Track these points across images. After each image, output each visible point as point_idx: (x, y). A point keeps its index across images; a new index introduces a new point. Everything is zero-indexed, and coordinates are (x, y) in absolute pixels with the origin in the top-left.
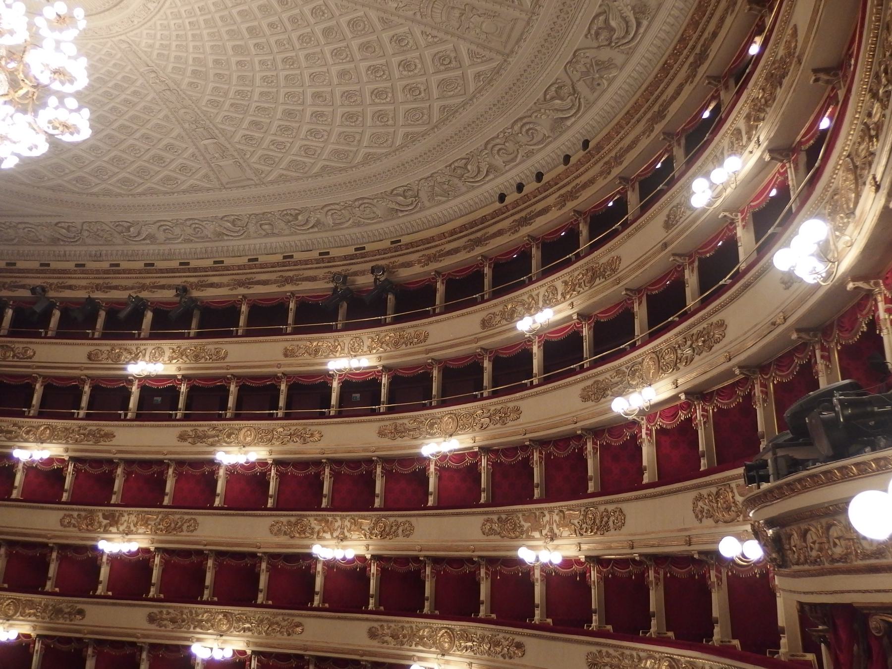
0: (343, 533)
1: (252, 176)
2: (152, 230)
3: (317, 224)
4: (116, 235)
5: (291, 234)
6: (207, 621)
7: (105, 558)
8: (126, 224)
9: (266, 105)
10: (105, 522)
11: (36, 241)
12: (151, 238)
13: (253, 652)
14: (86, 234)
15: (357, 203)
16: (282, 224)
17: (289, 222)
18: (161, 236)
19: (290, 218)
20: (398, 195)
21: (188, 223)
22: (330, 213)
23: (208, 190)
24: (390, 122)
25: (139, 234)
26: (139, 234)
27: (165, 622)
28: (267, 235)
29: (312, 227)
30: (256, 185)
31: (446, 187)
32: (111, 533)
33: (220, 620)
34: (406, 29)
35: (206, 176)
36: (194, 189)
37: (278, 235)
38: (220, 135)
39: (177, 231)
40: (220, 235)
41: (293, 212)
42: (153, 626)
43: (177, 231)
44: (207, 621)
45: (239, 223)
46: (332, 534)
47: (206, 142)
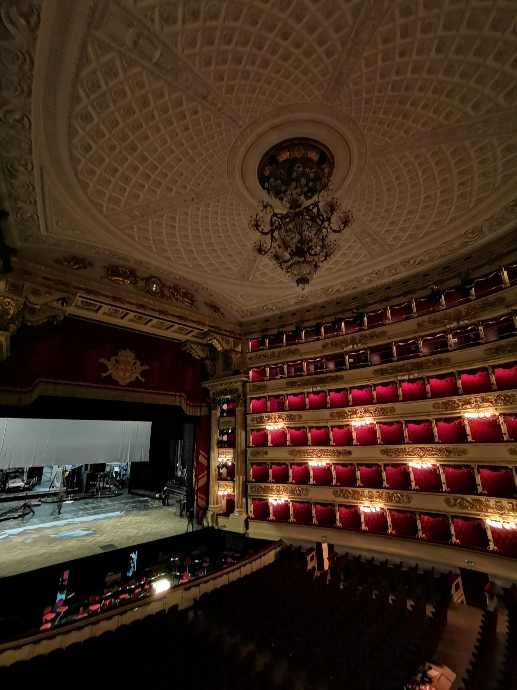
0: (478, 404)
1: (388, 249)
2: (338, 287)
3: (421, 261)
4: (322, 294)
5: (406, 271)
6: (412, 452)
7: (353, 429)
8: (327, 288)
9: (399, 212)
10: (350, 413)
11: (290, 306)
12: (338, 291)
13: (440, 465)
14: (309, 297)
15: (443, 245)
16: (402, 267)
17: (405, 265)
18: (342, 289)
19: (406, 263)
20: (468, 234)
21: (355, 280)
22: (427, 255)
23: (365, 262)
24: (468, 196)
25: (332, 291)
26: (332, 291)
27: (390, 454)
28: (394, 275)
29: (418, 264)
30: (389, 252)
31: (500, 220)
32: (353, 418)
33: (418, 451)
34: (487, 141)
35: (365, 256)
36: (359, 263)
37: (399, 273)
38: (374, 234)
39: (350, 285)
40: (370, 281)
41: (407, 260)
42: (385, 456)
43: (350, 285)
44: (412, 452)
45: (379, 273)
46: (471, 406)
47: (367, 240)
